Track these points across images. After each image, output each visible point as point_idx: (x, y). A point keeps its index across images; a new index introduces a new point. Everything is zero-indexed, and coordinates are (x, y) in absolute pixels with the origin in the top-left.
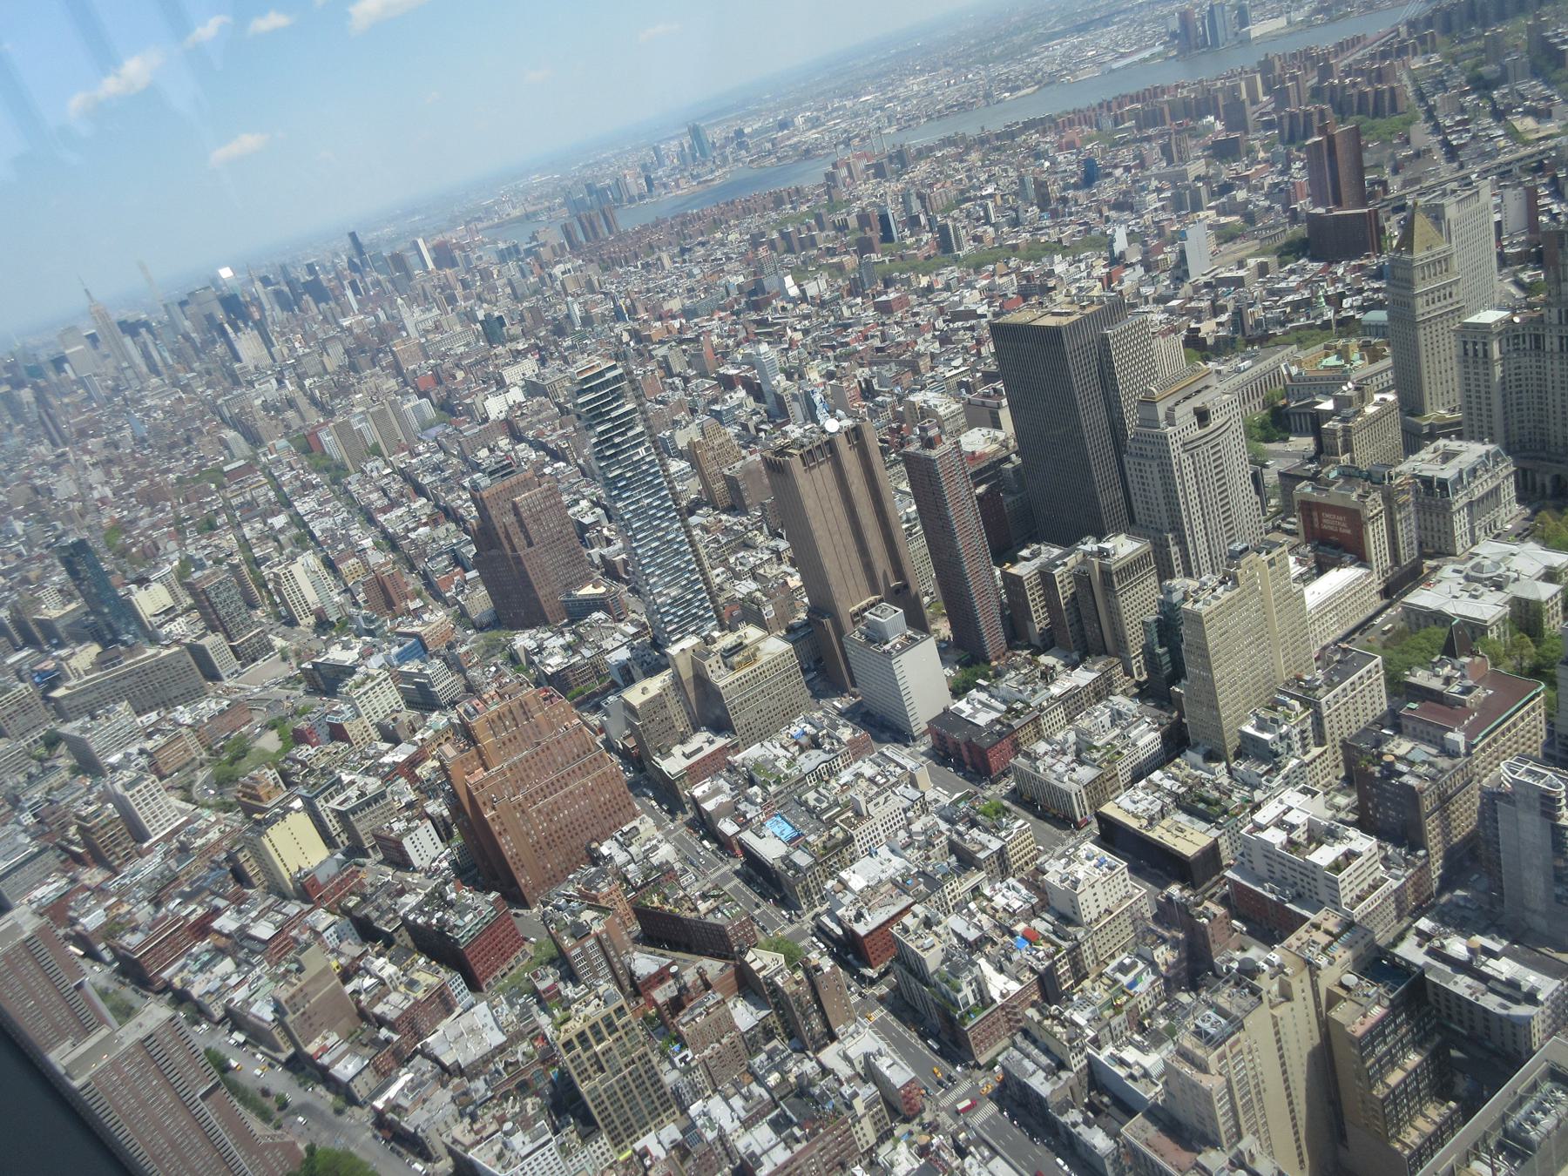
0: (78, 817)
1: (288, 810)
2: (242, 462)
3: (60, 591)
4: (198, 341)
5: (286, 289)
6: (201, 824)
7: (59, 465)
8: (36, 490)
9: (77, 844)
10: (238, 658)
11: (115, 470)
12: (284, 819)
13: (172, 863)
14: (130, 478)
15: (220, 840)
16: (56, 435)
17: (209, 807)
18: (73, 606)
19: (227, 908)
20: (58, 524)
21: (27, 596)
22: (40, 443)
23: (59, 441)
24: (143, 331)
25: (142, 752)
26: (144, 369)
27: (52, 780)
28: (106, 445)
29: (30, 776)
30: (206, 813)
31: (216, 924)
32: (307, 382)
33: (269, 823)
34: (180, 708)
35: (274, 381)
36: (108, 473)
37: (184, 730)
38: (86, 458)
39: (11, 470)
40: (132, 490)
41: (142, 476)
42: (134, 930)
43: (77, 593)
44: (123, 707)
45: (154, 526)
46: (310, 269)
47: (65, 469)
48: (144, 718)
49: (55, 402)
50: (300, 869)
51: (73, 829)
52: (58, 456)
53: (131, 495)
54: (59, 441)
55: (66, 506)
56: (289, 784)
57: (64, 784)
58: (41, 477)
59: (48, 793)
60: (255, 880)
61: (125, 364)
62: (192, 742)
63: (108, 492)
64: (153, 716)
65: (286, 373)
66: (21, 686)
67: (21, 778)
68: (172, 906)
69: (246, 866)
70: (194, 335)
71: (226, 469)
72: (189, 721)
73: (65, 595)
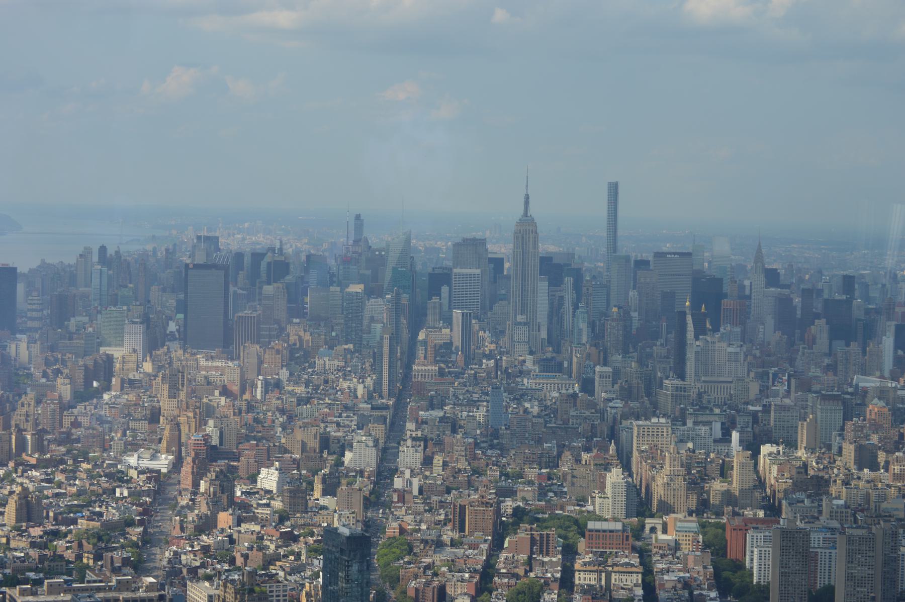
2: (619, 526)
4: (636, 324)
5: (797, 301)
8: (325, 442)
22: (362, 379)
24: (569, 281)
26: (544, 334)
28: (442, 419)
32: (766, 449)
35: (717, 427)
36: (428, 461)
39: (307, 401)
41: (470, 484)
46: (848, 282)
53: (442, 504)
61: (520, 318)
63: (416, 483)
65: (740, 420)
70: (635, 314)
71: (591, 525)
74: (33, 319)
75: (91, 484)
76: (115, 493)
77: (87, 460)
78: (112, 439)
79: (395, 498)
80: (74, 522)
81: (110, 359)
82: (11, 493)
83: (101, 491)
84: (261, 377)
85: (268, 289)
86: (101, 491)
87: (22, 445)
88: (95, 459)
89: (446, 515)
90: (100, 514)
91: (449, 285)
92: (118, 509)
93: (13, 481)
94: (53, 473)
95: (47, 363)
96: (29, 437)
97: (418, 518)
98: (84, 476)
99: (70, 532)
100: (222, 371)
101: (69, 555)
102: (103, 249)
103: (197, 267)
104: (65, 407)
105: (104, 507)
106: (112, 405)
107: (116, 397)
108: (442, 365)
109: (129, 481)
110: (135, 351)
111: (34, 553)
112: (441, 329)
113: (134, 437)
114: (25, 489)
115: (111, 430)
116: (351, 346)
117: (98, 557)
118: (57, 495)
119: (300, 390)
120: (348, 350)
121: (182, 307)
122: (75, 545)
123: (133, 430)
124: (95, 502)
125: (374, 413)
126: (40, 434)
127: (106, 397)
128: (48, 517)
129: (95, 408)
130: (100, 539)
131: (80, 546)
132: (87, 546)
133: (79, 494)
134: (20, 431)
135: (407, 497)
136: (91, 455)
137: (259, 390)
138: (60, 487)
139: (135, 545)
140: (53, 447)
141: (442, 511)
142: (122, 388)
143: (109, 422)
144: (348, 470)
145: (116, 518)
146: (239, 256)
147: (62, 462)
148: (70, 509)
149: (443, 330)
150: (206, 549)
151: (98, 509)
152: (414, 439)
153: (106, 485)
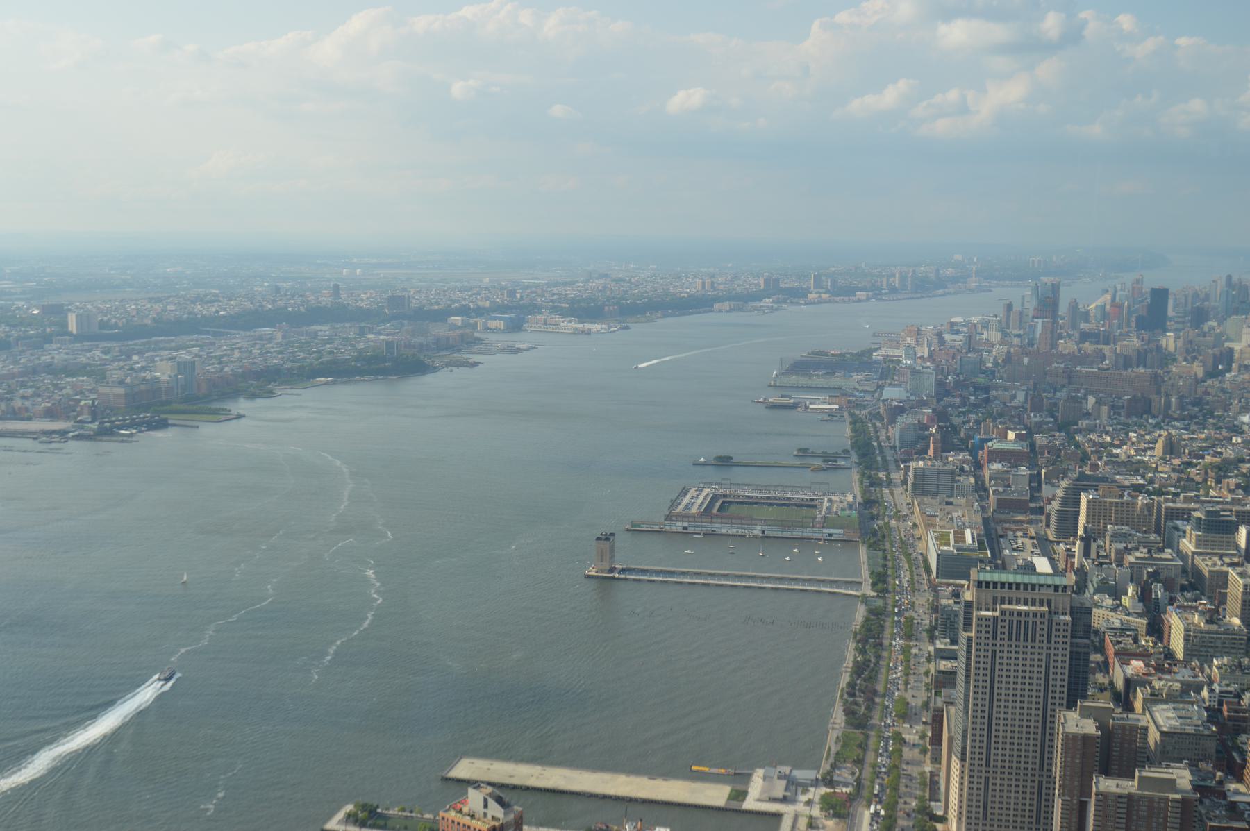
75: (1215, 433)
76: (1231, 439)
77: (1213, 417)
78: (1231, 404)
80: (1203, 457)
81: (1231, 351)
82: (1160, 435)
83: (1222, 438)
86: (1222, 438)
87: (1168, 405)
88: (1219, 417)
90: (1221, 453)
92: (1233, 450)
93: (1161, 428)
94: (1189, 424)
95: (1188, 352)
96: (1173, 400)
98: (1210, 427)
99: (1200, 463)
101: (1199, 479)
105: (1223, 449)
107: (1235, 376)
109: (1243, 432)
111: (1174, 476)
114: (1170, 434)
115: (1230, 398)
117: (1218, 481)
118: (1192, 439)
122: (1203, 472)
123: (1247, 399)
124: (1218, 445)
126: (1181, 398)
127: (1228, 375)
128: (1184, 453)
129: (1220, 383)
130: (1220, 469)
131: (1206, 473)
132: (1211, 474)
133: (1206, 440)
134: (1168, 396)
136: (1216, 414)
138: (1193, 433)
140: (1190, 407)
142: (1239, 371)
143: (1230, 393)
145: (1232, 456)
147: (1196, 417)
148: (1201, 448)
151: (1219, 450)
153: (1226, 434)
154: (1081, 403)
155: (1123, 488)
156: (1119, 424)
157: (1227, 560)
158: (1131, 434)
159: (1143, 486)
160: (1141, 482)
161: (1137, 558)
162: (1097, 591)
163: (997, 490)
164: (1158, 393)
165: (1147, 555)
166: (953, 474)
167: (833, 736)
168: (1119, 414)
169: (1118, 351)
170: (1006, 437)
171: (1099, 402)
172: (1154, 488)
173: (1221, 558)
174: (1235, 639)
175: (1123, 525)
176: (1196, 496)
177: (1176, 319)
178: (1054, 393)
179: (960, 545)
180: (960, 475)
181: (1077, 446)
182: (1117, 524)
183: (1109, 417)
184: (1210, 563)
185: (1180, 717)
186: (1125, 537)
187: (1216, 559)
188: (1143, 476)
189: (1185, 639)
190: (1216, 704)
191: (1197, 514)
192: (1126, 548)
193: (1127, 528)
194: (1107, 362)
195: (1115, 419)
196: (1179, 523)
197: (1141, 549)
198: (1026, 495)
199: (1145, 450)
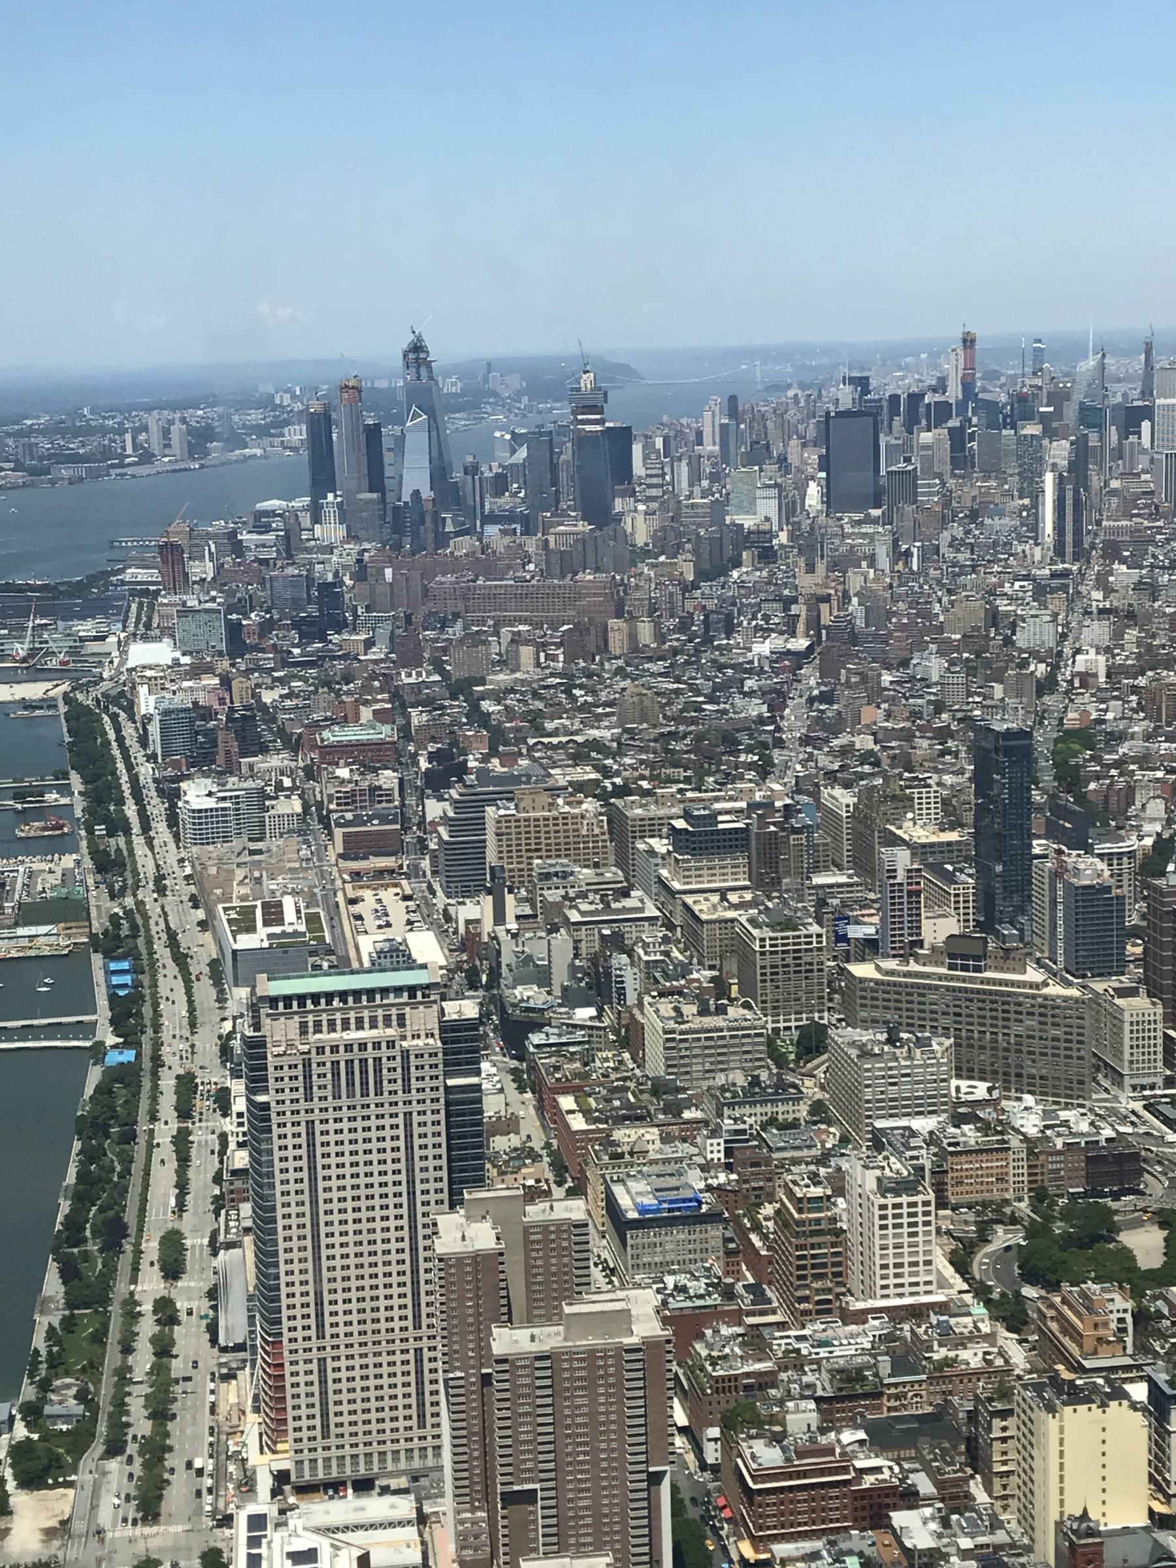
0: (790, 1194)
1: (1119, 1395)
3: (945, 802)
6: (963, 1324)
7: (1054, 591)
8: (994, 617)
9: (764, 1237)
10: (1167, 1064)
11: (1132, 634)
12: (1103, 1406)
13: (885, 1364)
14: (1149, 660)
15: (977, 1374)
16: (1069, 538)
17: (988, 1303)
18: (953, 836)
19: (929, 1500)
20: (998, 690)
21: (895, 788)
23: (1069, 549)
25: (932, 1139)
27: (781, 1108)
28: (1139, 586)
29: (755, 1082)
30: (979, 1310)
31: (899, 1518)
33: (1076, 1396)
34: (1029, 1100)
36: (1118, 635)
37: (1015, 1142)
38: (1097, 595)
39: (974, 569)
40: (1142, 681)
42: (777, 1439)
43: (969, 817)
44: (940, 1045)
45: (1145, 761)
47: (1057, 602)
48: (964, 1084)
49: (1095, 481)
50: (1085, 1516)
51: (768, 1210)
52: (1054, 575)
54: (1069, 549)
55: (1024, 664)
56: (1142, 1348)
57: (795, 1124)
58: (1011, 599)
59: (764, 1126)
60: (997, 1482)
62: (1017, 1169)
63: (1100, 663)
64: (981, 1090)
66: (815, 929)
67: (740, 1079)
68: (848, 1436)
69: (997, 1446)
72: (1032, 1132)
73: (950, 817)
74: (650, 486)
79: (1077, 684)
84: (918, 544)
85: (926, 437)
88: (719, 648)
89: (1139, 703)
91: (1152, 420)
97: (1103, 706)
99: (690, 733)
100: (871, 537)
102: (733, 399)
103: (840, 414)
104: (688, 588)
106: (741, 585)
108: (1139, 520)
109: (761, 671)
110: (767, 519)
112: (1138, 475)
113: (767, 618)
116: (1026, 501)
119: (964, 557)
120: (1024, 507)
121: (824, 463)
125: (1055, 583)
127: (735, 574)
135: (1091, 680)
137: (915, 559)
139: (765, 745)
141: (1134, 698)
144: (1021, 651)
146: (895, 399)
149: (1144, 477)
150: (846, 751)
152: (1102, 611)
154: (485, 643)
155: (555, 791)
156: (552, 675)
157: (733, 898)
158: (577, 692)
159: (597, 782)
160: (593, 776)
161: (583, 913)
162: (518, 981)
163: (343, 817)
164: (619, 614)
165: (600, 906)
166: (263, 795)
167: (42, 1322)
168: (554, 658)
169: (552, 545)
170: (357, 719)
171: (517, 639)
172: (613, 784)
173: (724, 898)
174: (749, 1036)
175: (559, 856)
176: (680, 791)
177: (649, 481)
178: (442, 628)
179: (277, 930)
180: (276, 798)
181: (483, 719)
182: (549, 857)
183: (538, 665)
184: (705, 908)
185: (657, 1190)
186: (564, 878)
187: (715, 898)
188: (597, 768)
189: (666, 1049)
190: (722, 1155)
191: (680, 824)
192: (566, 897)
193: (565, 861)
194: (531, 567)
195: (548, 667)
196: (654, 842)
197: (591, 896)
198: (394, 822)
199: (599, 718)
